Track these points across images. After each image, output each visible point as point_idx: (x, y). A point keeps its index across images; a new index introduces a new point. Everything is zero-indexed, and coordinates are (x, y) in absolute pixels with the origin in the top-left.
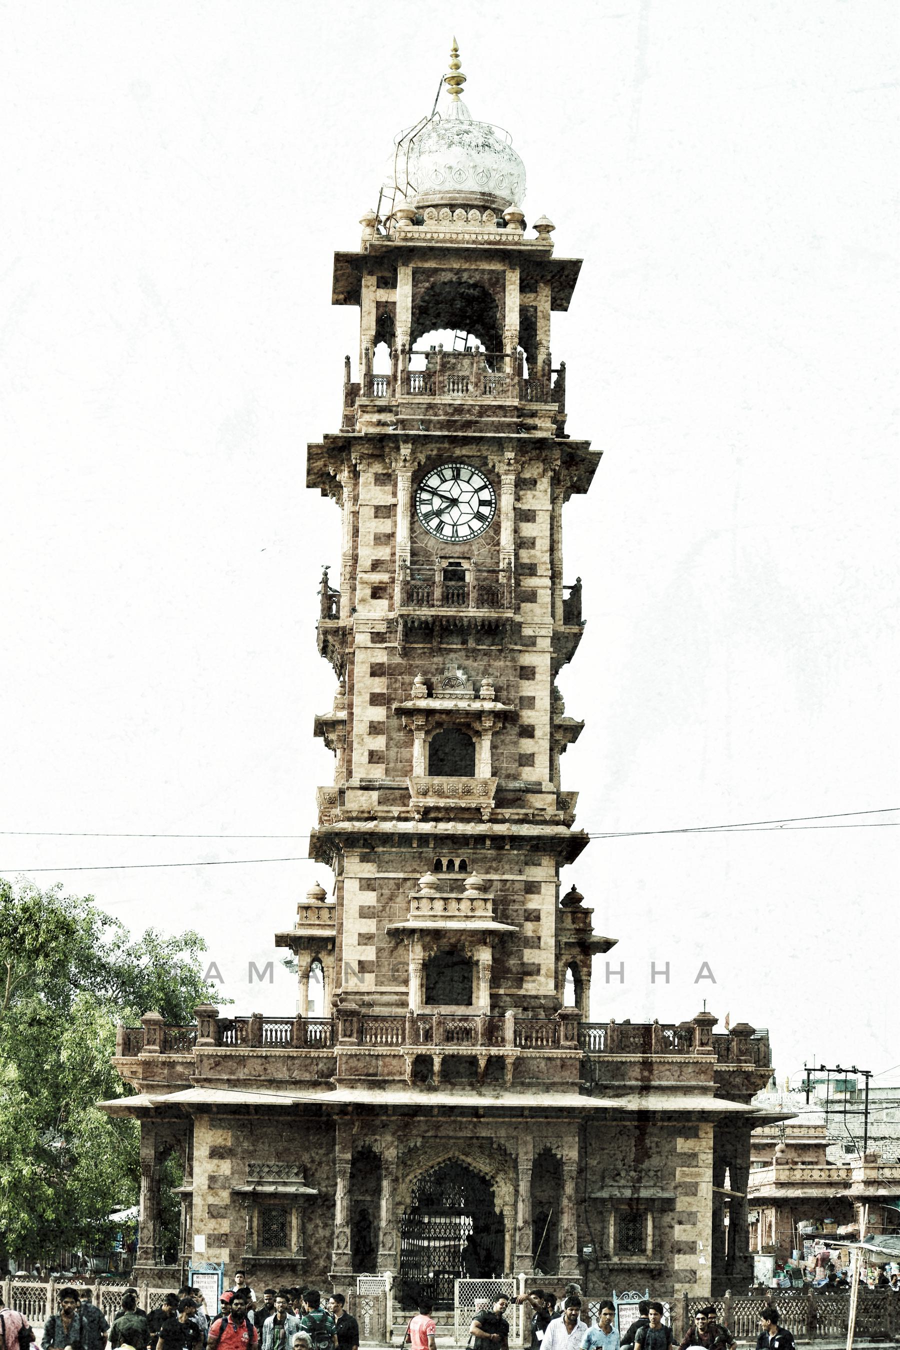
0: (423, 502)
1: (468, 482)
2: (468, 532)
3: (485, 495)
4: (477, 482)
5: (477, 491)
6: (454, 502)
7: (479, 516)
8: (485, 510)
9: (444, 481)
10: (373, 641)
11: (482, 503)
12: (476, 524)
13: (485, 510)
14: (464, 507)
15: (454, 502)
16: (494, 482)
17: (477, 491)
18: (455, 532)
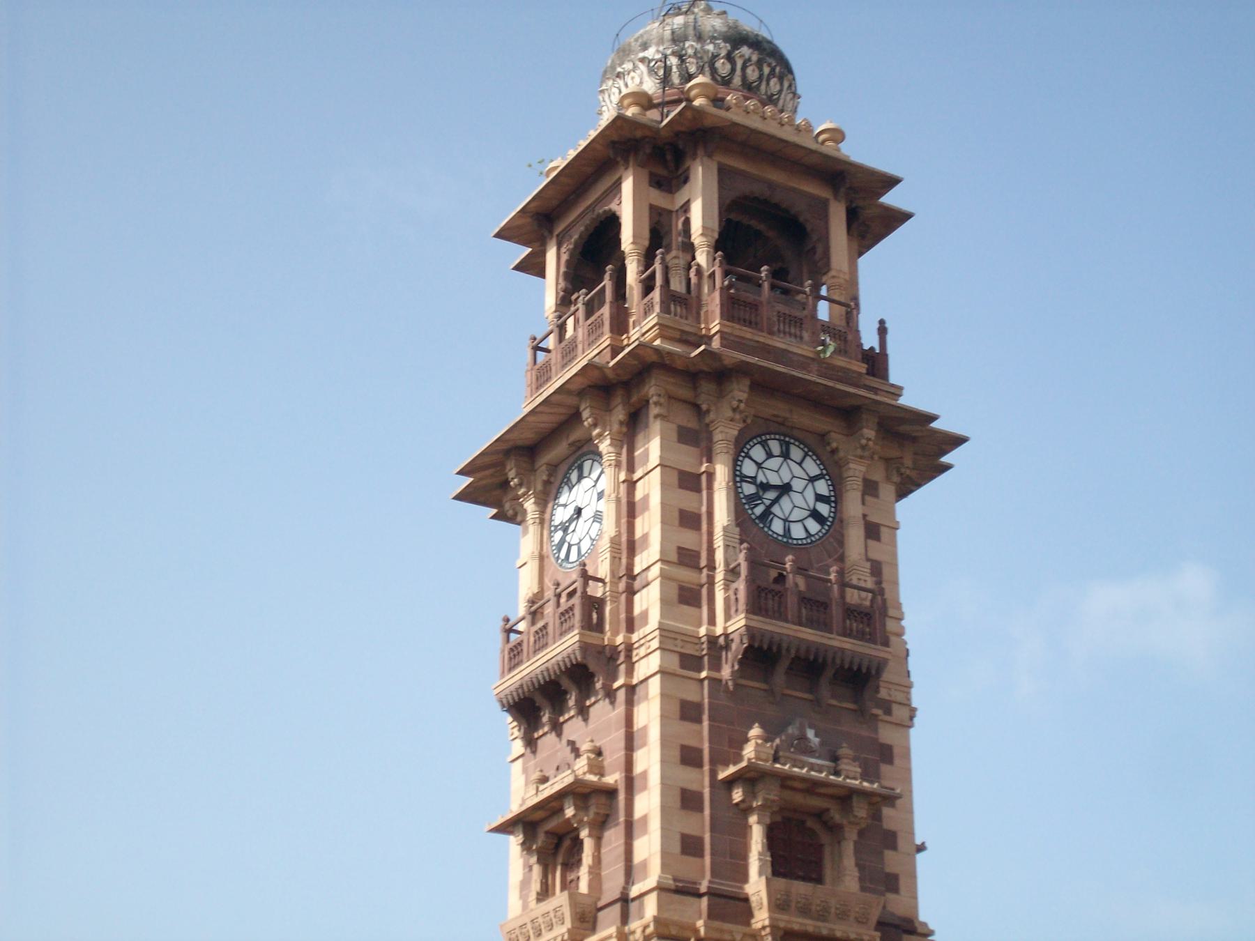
0: (744, 478)
1: (800, 464)
2: (802, 534)
3: (822, 487)
4: (812, 468)
5: (812, 480)
6: (785, 489)
7: (815, 515)
8: (824, 509)
9: (770, 455)
10: (683, 666)
11: (819, 498)
12: (814, 527)
13: (824, 509)
14: (797, 499)
15: (785, 489)
16: (833, 472)
17: (812, 480)
18: (787, 531)
